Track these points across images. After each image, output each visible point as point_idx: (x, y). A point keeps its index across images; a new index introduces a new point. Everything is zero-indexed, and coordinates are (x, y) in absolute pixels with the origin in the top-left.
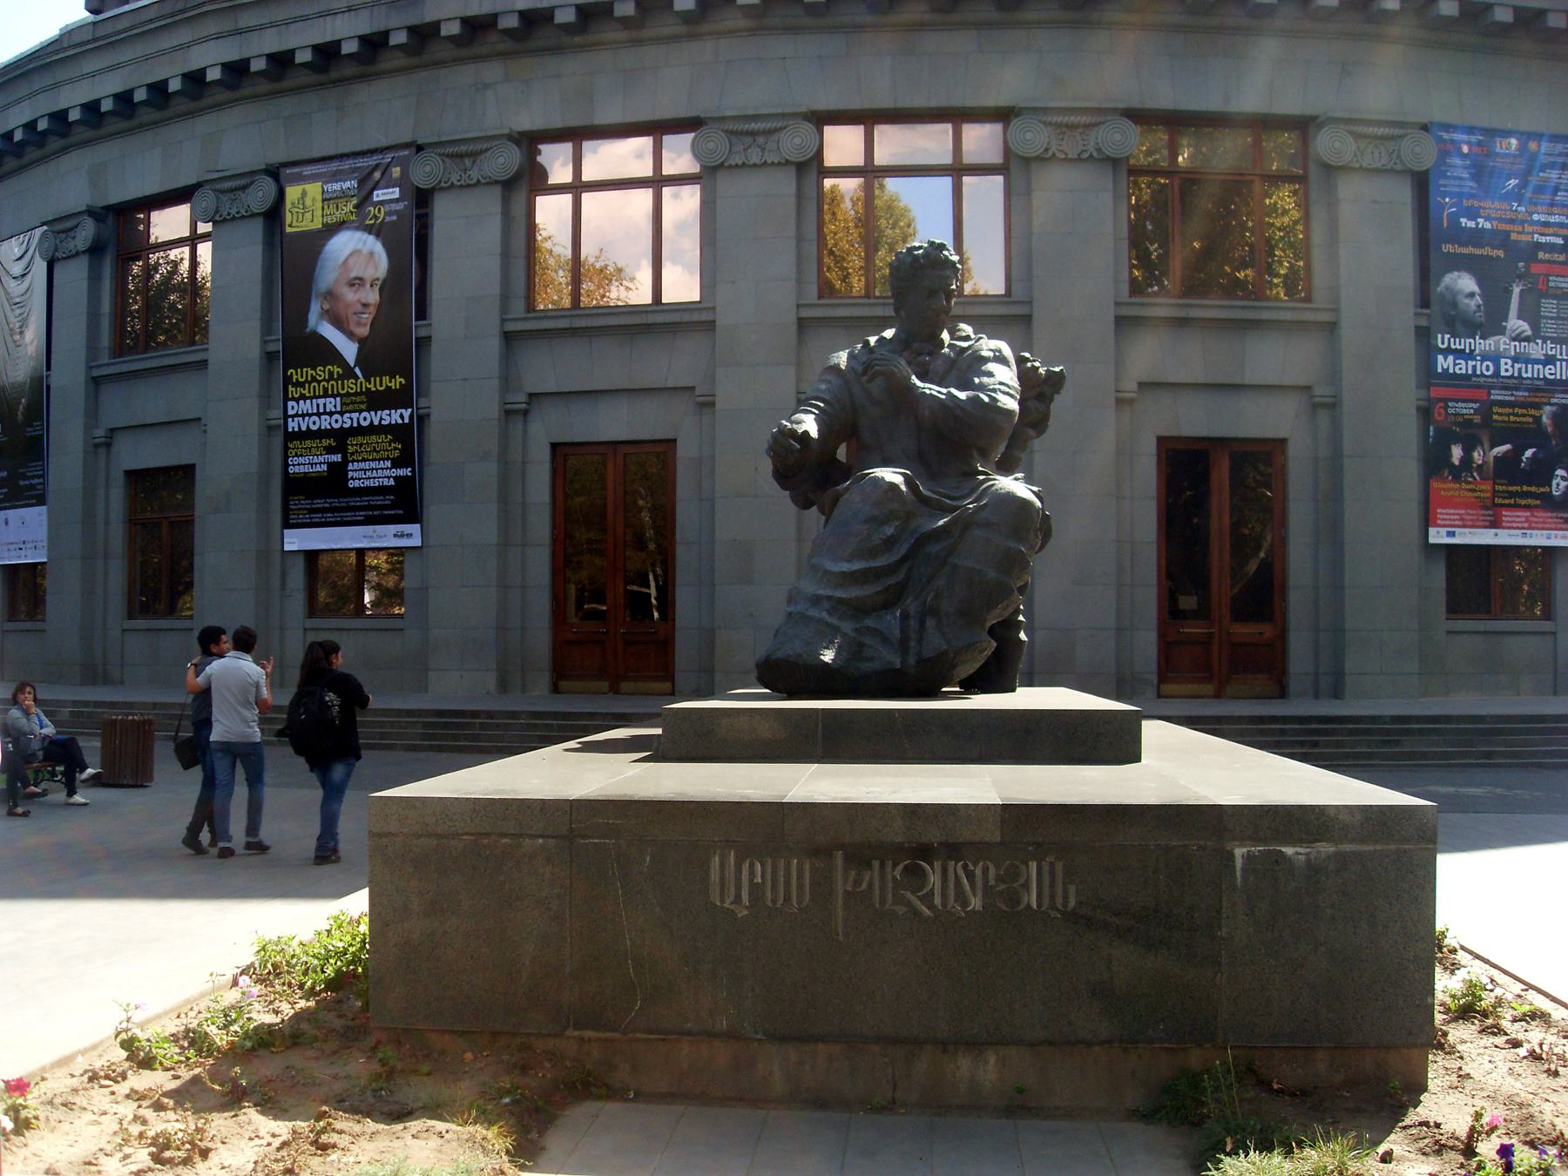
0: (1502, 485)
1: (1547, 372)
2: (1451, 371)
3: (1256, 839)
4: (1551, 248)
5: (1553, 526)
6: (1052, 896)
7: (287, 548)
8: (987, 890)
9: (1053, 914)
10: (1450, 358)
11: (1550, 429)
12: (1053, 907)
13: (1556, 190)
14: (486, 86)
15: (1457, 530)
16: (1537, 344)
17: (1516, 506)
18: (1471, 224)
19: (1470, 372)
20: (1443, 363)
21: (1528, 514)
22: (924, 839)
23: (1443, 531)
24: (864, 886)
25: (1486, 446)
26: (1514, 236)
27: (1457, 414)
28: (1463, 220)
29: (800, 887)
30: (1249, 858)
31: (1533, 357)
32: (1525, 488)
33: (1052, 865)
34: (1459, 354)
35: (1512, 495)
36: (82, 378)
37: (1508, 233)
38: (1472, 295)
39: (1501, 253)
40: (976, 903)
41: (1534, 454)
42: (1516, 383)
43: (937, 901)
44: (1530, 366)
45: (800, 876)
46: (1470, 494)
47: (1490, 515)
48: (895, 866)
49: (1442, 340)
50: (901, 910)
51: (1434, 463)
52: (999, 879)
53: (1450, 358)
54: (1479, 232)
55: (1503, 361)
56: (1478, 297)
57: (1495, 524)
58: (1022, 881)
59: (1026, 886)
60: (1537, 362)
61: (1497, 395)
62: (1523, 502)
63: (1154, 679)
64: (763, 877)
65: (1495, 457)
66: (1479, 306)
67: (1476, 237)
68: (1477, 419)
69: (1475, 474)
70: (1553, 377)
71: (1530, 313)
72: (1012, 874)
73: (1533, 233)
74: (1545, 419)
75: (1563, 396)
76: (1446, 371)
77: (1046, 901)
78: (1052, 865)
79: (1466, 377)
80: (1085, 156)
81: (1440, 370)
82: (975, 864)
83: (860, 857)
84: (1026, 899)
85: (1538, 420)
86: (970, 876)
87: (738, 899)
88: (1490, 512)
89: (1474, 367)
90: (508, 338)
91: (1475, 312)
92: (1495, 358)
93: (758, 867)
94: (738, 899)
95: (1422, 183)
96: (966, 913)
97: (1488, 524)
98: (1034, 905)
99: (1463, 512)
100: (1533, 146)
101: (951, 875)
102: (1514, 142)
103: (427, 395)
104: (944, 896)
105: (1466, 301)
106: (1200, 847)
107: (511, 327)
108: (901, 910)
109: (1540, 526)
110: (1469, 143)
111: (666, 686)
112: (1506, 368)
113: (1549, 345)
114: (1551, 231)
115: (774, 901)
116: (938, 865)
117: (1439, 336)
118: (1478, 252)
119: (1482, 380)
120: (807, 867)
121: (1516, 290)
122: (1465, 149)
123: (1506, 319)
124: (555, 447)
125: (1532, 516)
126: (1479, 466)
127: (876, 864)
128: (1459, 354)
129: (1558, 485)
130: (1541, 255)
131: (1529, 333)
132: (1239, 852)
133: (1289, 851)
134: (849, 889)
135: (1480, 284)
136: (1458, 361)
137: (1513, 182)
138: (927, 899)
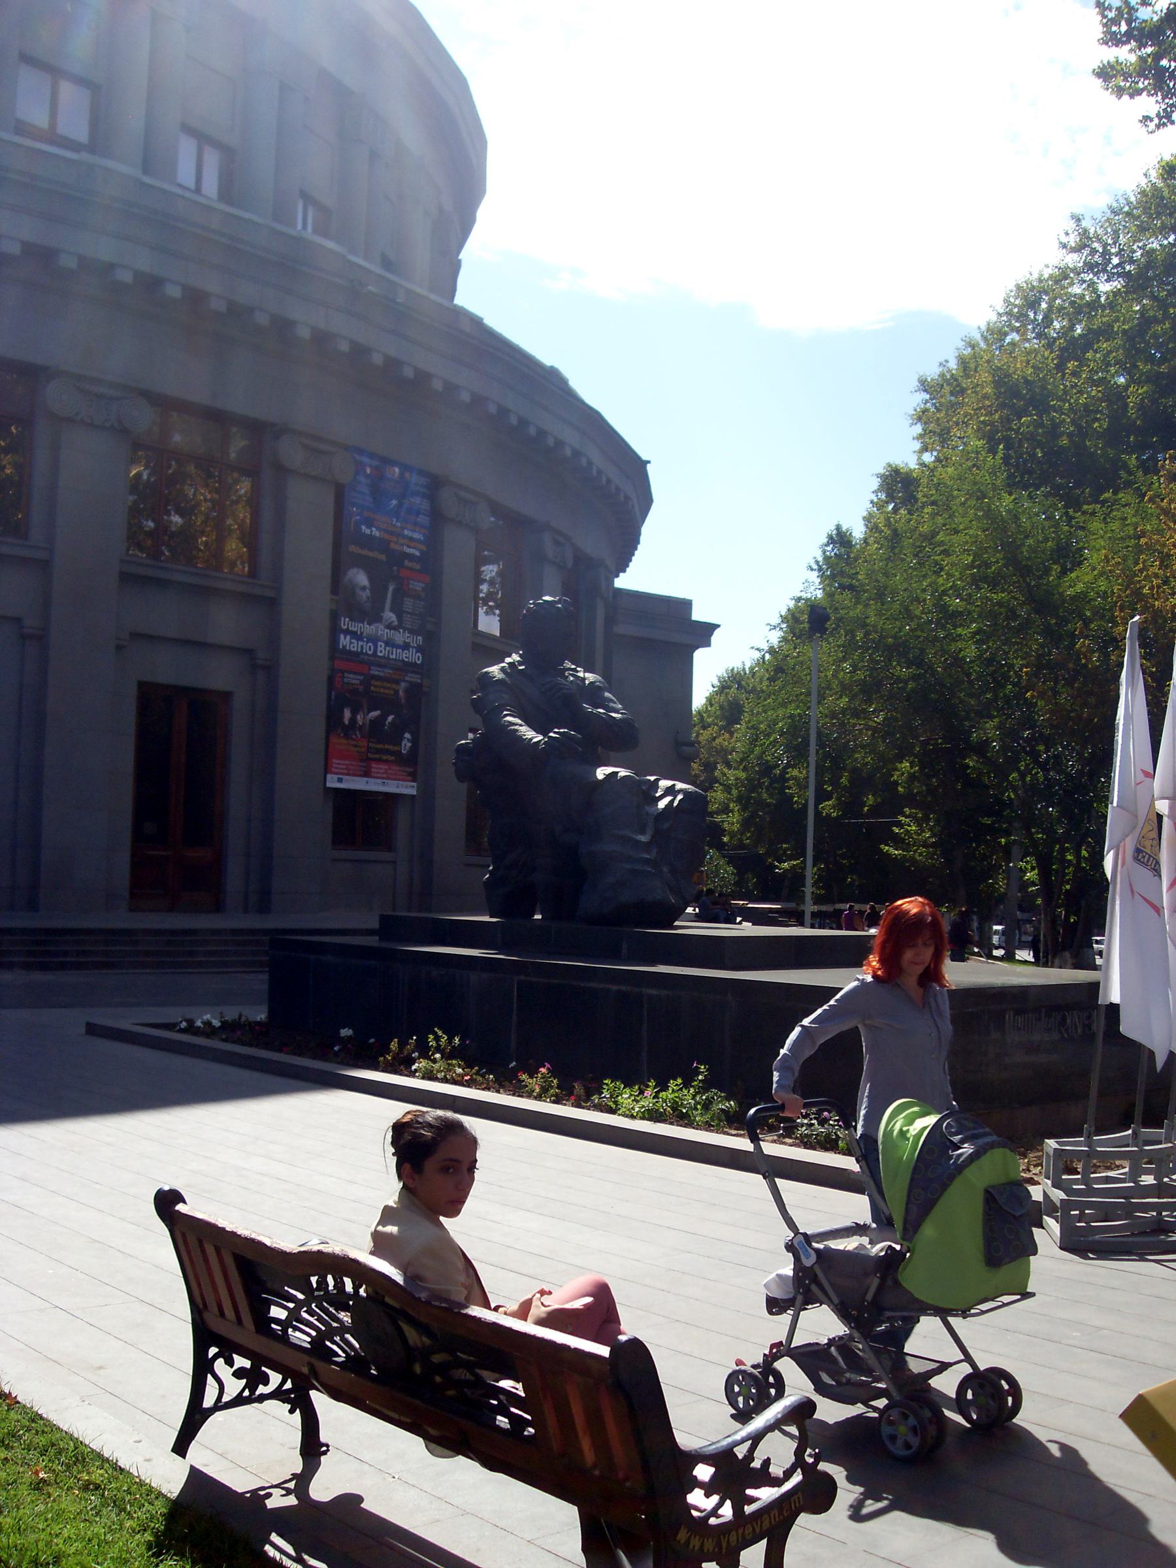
0: (374, 743)
1: (404, 655)
2: (348, 648)
4: (411, 557)
5: (401, 777)
10: (348, 637)
11: (403, 701)
13: (418, 513)
15: (344, 777)
16: (400, 632)
17: (380, 761)
18: (368, 531)
19: (359, 650)
20: (344, 641)
21: (386, 767)
23: (336, 777)
25: (366, 711)
26: (392, 545)
27: (348, 684)
28: (363, 527)
31: (397, 643)
32: (386, 746)
34: (354, 635)
35: (378, 751)
37: (389, 542)
38: (364, 588)
39: (383, 557)
41: (393, 719)
42: (384, 663)
44: (394, 650)
46: (354, 749)
47: (363, 766)
49: (345, 623)
51: (333, 721)
53: (348, 637)
54: (371, 537)
55: (379, 643)
56: (368, 591)
57: (367, 774)
60: (398, 647)
61: (375, 671)
62: (384, 757)
65: (370, 720)
66: (368, 598)
67: (369, 542)
68: (361, 689)
69: (358, 733)
70: (407, 660)
71: (397, 609)
73: (402, 545)
74: (401, 693)
75: (413, 675)
76: (344, 647)
79: (357, 654)
80: (108, 425)
81: (341, 647)
85: (397, 692)
88: (364, 764)
89: (362, 647)
91: (366, 602)
92: (374, 640)
95: (340, 493)
97: (362, 773)
99: (348, 762)
100: (407, 475)
102: (397, 470)
105: (361, 593)
109: (393, 777)
110: (371, 466)
112: (382, 650)
113: (407, 635)
114: (412, 544)
117: (343, 619)
118: (371, 554)
119: (366, 657)
121: (391, 588)
122: (368, 471)
123: (383, 610)
125: (389, 769)
126: (361, 727)
128: (354, 635)
129: (405, 745)
130: (406, 563)
131: (396, 623)
135: (371, 579)
136: (353, 641)
137: (394, 502)
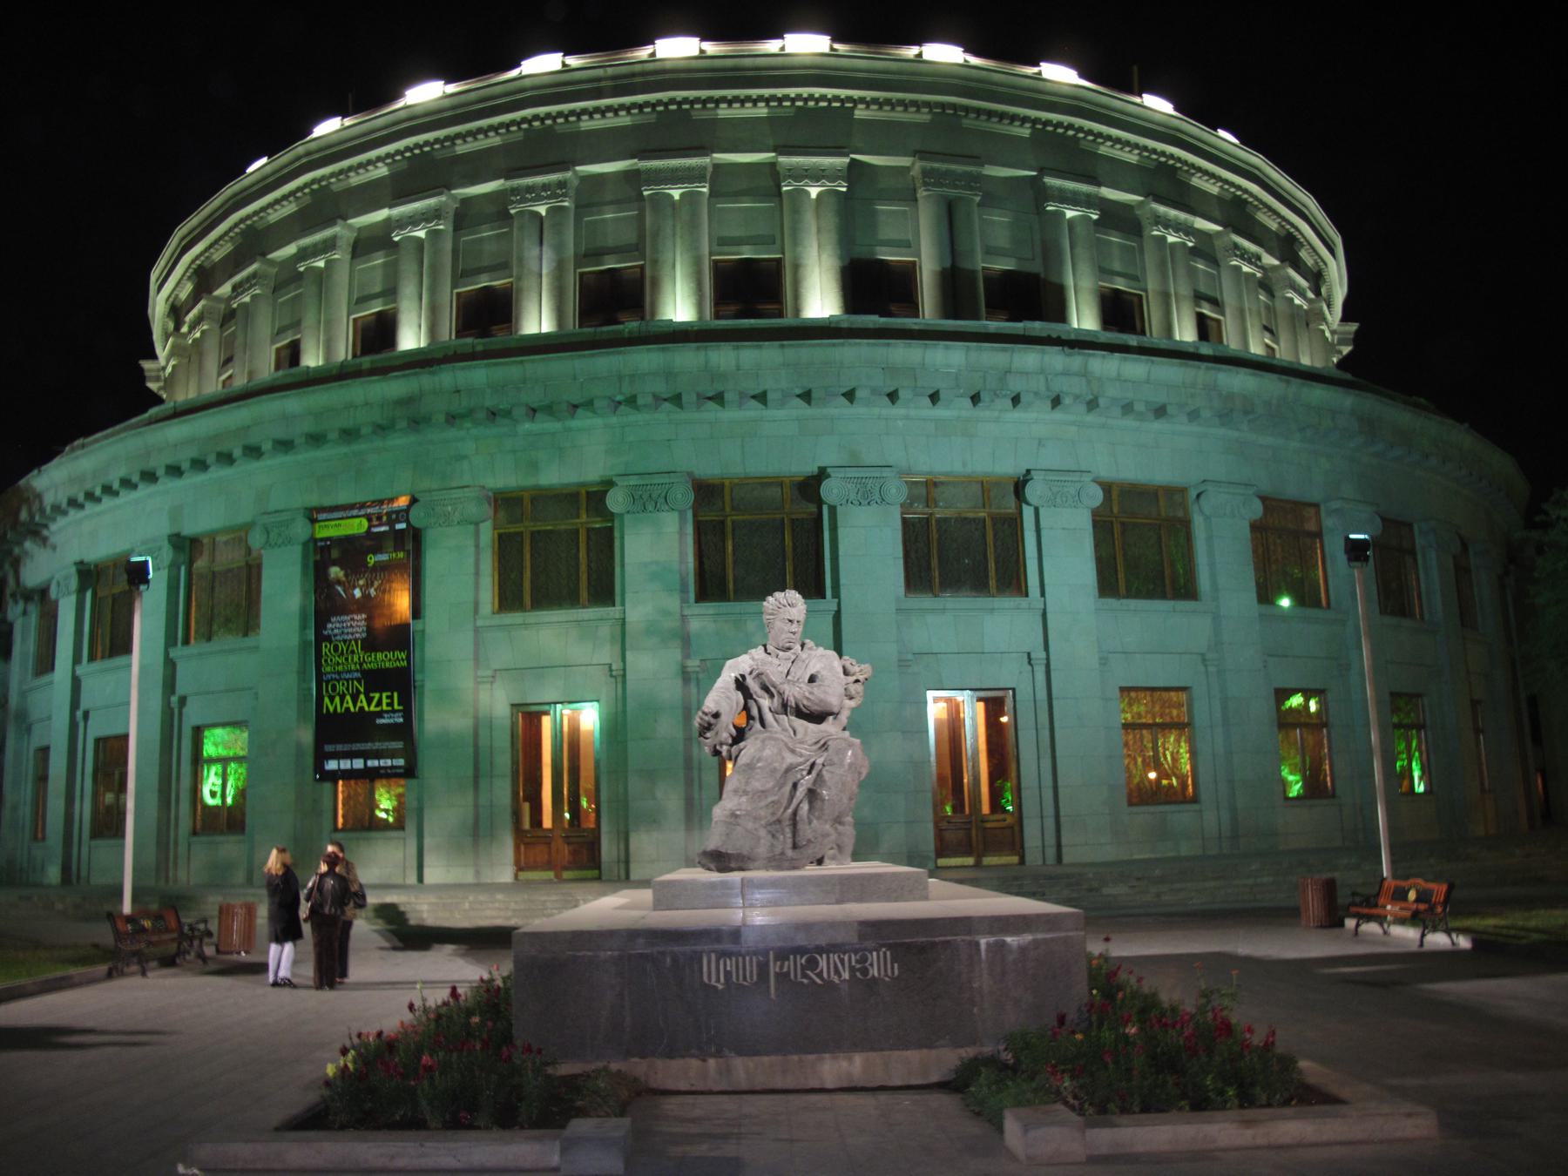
3: (991, 933)
6: (886, 970)
8: (852, 969)
9: (887, 979)
12: (886, 975)
14: (464, 457)
22: (817, 943)
24: (785, 970)
29: (751, 972)
30: (988, 944)
33: (885, 953)
36: (161, 659)
40: (846, 975)
43: (825, 975)
45: (751, 966)
48: (801, 958)
50: (805, 981)
52: (857, 962)
58: (869, 962)
59: (872, 965)
63: (932, 855)
64: (731, 967)
72: (863, 960)
77: (882, 972)
78: (885, 953)
82: (844, 954)
83: (782, 955)
84: (871, 972)
86: (842, 961)
87: (718, 980)
90: (476, 630)
93: (728, 962)
94: (718, 980)
96: (841, 981)
98: (876, 974)
101: (831, 962)
104: (829, 972)
106: (963, 941)
107: (480, 623)
108: (805, 981)
111: (597, 872)
115: (738, 979)
116: (824, 956)
120: (754, 959)
127: (792, 957)
132: (983, 942)
133: (1009, 939)
134: (777, 970)
138: (820, 975)
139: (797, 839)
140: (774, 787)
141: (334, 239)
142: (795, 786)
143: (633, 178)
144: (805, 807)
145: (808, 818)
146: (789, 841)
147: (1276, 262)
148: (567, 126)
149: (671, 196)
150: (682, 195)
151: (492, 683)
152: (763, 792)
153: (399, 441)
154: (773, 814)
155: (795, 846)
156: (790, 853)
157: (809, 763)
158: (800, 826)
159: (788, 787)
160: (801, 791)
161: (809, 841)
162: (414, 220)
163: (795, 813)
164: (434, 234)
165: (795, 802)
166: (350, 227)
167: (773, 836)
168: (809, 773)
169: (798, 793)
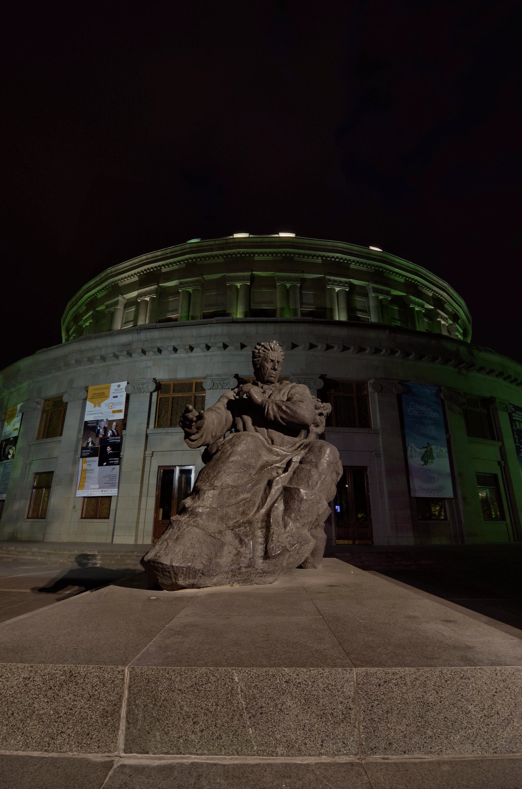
7: (77, 496)
103: (124, 451)
124: (159, 466)
139: (271, 546)
140: (246, 483)
141: (118, 301)
142: (270, 484)
143: (222, 282)
144: (280, 506)
145: (283, 519)
146: (260, 549)
147: (452, 322)
148: (201, 262)
149: (236, 286)
150: (241, 286)
151: (152, 457)
152: (233, 487)
153: (123, 360)
154: (243, 513)
155: (266, 556)
156: (260, 562)
157: (285, 461)
158: (274, 528)
159: (263, 484)
160: (276, 488)
161: (285, 550)
162: (145, 294)
163: (268, 514)
164: (152, 299)
165: (269, 501)
166: (124, 298)
167: (241, 541)
168: (285, 470)
169: (273, 491)
